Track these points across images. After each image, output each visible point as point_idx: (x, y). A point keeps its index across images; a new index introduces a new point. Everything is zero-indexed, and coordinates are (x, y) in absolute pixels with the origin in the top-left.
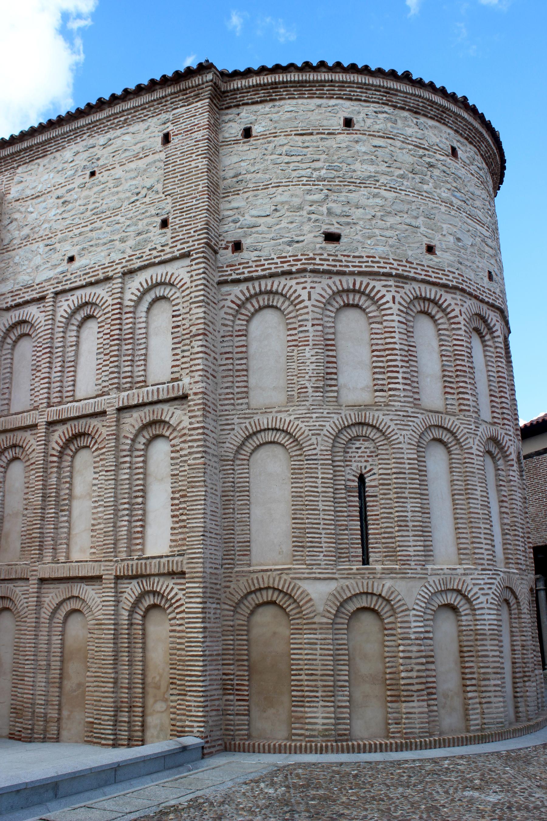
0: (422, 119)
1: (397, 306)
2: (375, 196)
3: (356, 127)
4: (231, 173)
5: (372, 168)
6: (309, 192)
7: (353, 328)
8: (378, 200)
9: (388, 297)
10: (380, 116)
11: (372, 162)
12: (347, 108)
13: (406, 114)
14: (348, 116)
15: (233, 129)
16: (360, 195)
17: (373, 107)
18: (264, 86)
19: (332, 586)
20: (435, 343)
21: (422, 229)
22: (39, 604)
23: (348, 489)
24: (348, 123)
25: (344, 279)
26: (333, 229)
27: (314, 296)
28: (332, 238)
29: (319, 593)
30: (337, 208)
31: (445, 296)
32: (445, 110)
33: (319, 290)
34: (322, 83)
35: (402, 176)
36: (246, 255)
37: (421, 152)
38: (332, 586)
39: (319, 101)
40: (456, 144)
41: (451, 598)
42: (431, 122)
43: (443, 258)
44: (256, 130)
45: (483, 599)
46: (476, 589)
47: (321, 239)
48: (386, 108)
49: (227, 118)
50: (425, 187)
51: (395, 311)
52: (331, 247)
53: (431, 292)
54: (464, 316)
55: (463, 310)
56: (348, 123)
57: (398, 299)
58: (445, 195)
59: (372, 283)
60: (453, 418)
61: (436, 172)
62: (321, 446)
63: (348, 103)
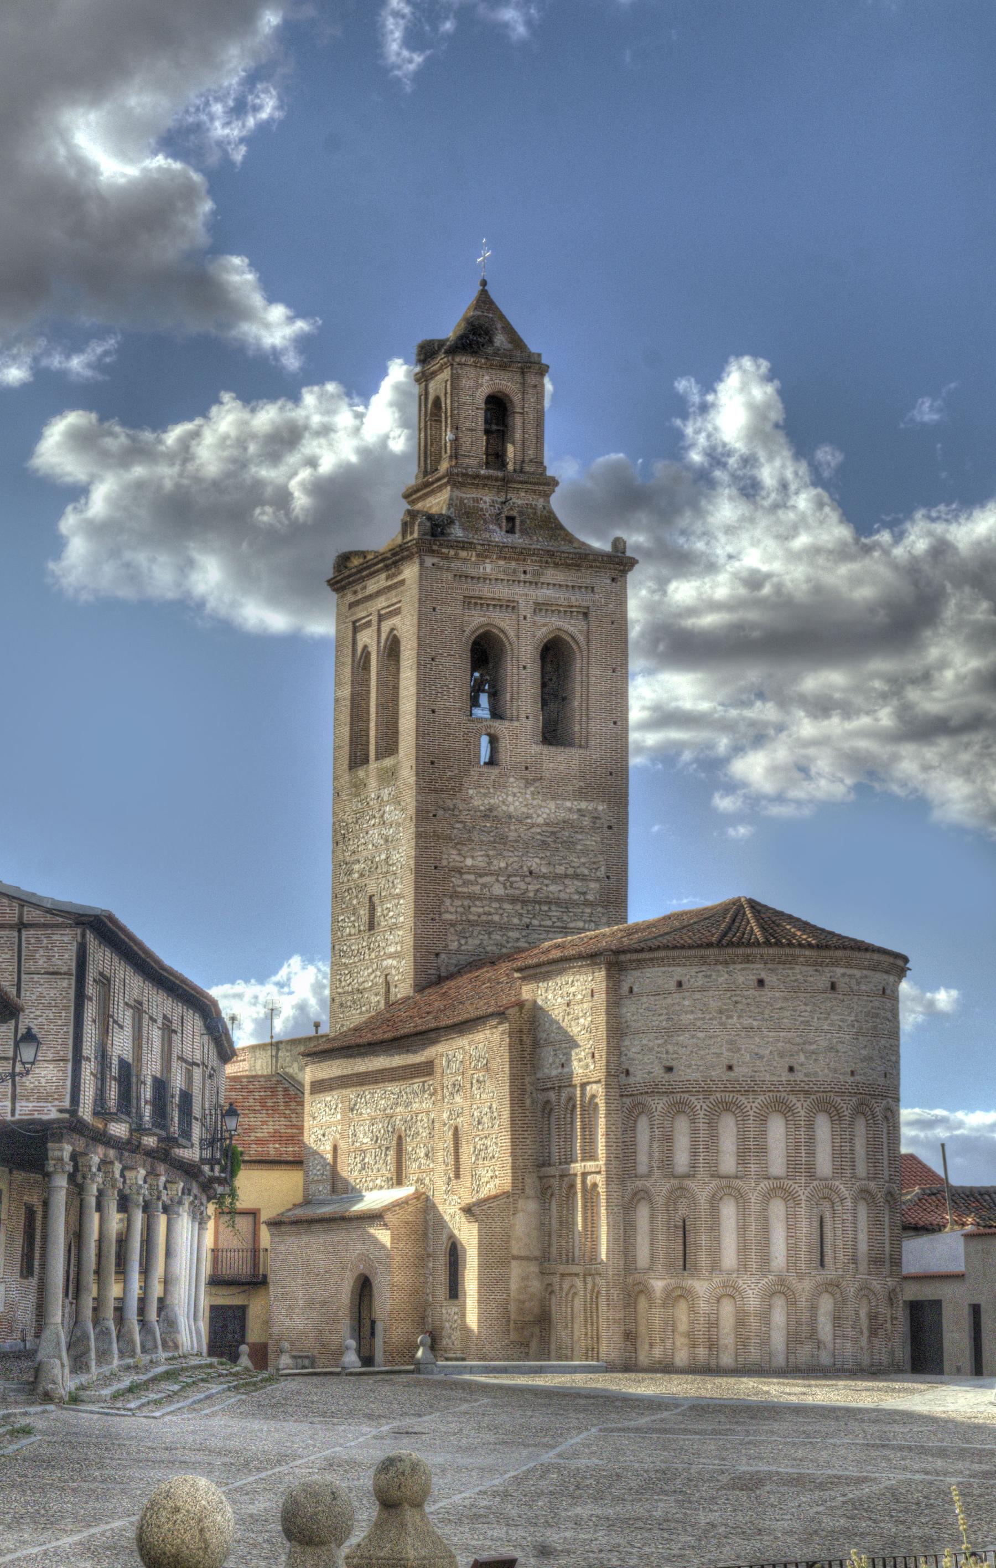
0: (731, 967)
1: (703, 1112)
2: (693, 1037)
3: (684, 987)
4: (624, 1020)
5: (691, 1017)
6: (657, 1038)
7: (682, 1126)
8: (695, 1040)
9: (698, 1107)
10: (700, 974)
11: (692, 1012)
12: (679, 972)
13: (720, 967)
14: (679, 979)
15: (625, 989)
16: (683, 1038)
17: (696, 969)
18: (634, 961)
19: (665, 1282)
20: (735, 1130)
21: (726, 1053)
22: (561, 1289)
23: (676, 1226)
24: (680, 984)
25: (674, 1095)
26: (668, 1064)
27: (659, 1109)
28: (669, 1069)
29: (658, 1285)
30: (670, 1048)
31: (740, 1098)
32: (749, 955)
33: (662, 1105)
34: (663, 959)
35: (711, 1019)
36: (631, 1080)
37: (729, 994)
38: (665, 1282)
39: (664, 969)
40: (763, 975)
41: (729, 1290)
42: (739, 967)
43: (739, 1071)
44: (635, 990)
45: (751, 1292)
46: (745, 1286)
47: (661, 1071)
48: (704, 968)
49: (622, 978)
50: (730, 1021)
51: (701, 1116)
52: (667, 1077)
53: (729, 1097)
54: (755, 1109)
55: (753, 1105)
56: (680, 984)
57: (705, 1107)
58: (747, 1021)
59: (691, 1098)
60: (738, 1181)
61: (740, 1006)
62: (660, 1201)
63: (679, 969)
